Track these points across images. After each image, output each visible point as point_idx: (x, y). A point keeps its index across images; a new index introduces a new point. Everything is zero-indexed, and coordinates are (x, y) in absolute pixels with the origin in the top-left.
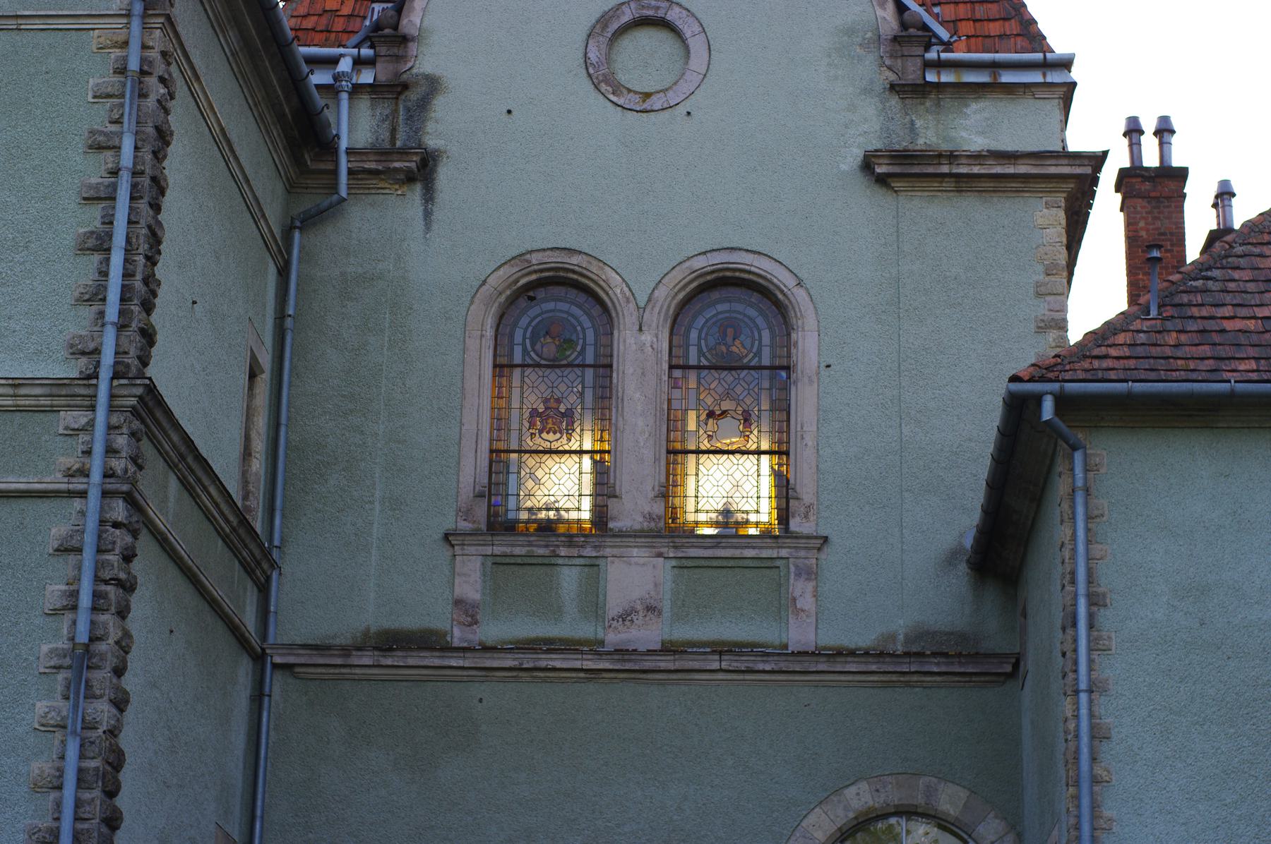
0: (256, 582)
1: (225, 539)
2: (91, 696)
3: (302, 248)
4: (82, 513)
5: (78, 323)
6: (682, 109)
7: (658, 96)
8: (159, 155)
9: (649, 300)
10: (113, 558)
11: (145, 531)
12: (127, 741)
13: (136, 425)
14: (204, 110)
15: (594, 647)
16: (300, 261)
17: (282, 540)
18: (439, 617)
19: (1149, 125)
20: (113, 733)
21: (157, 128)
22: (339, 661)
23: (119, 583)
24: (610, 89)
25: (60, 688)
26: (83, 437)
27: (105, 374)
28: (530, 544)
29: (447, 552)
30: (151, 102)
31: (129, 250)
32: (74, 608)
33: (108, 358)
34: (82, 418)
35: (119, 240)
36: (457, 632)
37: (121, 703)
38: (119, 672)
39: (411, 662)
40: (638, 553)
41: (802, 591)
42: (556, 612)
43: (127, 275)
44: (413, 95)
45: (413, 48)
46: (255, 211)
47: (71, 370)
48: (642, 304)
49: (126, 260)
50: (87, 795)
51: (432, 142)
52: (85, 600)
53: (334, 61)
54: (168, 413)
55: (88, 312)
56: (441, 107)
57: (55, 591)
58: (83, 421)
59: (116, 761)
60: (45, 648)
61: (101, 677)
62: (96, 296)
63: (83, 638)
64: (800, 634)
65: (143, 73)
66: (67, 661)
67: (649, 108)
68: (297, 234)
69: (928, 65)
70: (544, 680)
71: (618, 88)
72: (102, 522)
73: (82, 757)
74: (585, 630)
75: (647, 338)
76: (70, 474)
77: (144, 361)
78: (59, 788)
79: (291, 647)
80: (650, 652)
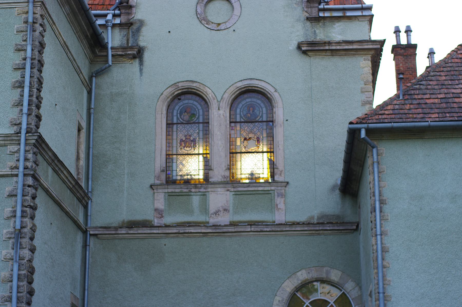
0: (83, 205)
1: (71, 190)
2: (22, 248)
3: (96, 84)
4: (17, 182)
5: (13, 114)
6: (232, 29)
7: (223, 24)
8: (40, 52)
9: (222, 98)
10: (28, 198)
11: (40, 188)
12: (35, 264)
13: (35, 150)
14: (57, 35)
15: (205, 224)
16: (95, 88)
17: (92, 189)
18: (149, 215)
19: (403, 29)
20: (30, 261)
21: (40, 43)
22: (113, 232)
23: (31, 207)
24: (205, 22)
25: (11, 245)
26: (16, 155)
27: (23, 132)
28: (181, 188)
29: (151, 192)
30: (37, 33)
31: (31, 87)
32: (15, 216)
33: (24, 126)
34: (15, 148)
35: (27, 84)
36: (156, 220)
37: (33, 250)
38: (32, 239)
39: (139, 232)
40: (220, 190)
41: (279, 201)
42: (190, 212)
43: (30, 96)
44: (135, 27)
45: (134, 10)
46: (78, 71)
47: (12, 130)
48: (219, 100)
49: (30, 91)
50: (21, 284)
51: (142, 44)
52: (19, 214)
53: (105, 16)
54: (47, 145)
55: (17, 110)
56: (144, 30)
57: (8, 210)
58: (16, 149)
59: (32, 271)
60: (5, 231)
61: (25, 241)
62: (19, 104)
63: (18, 227)
64: (279, 217)
65: (34, 23)
66: (13, 236)
67: (220, 29)
68: (94, 79)
69: (320, 10)
70: (188, 237)
71: (208, 22)
72: (24, 185)
73: (19, 270)
74: (202, 218)
75: (221, 112)
76: (12, 168)
77: (38, 127)
78: (11, 281)
79: (96, 228)
80: (226, 226)
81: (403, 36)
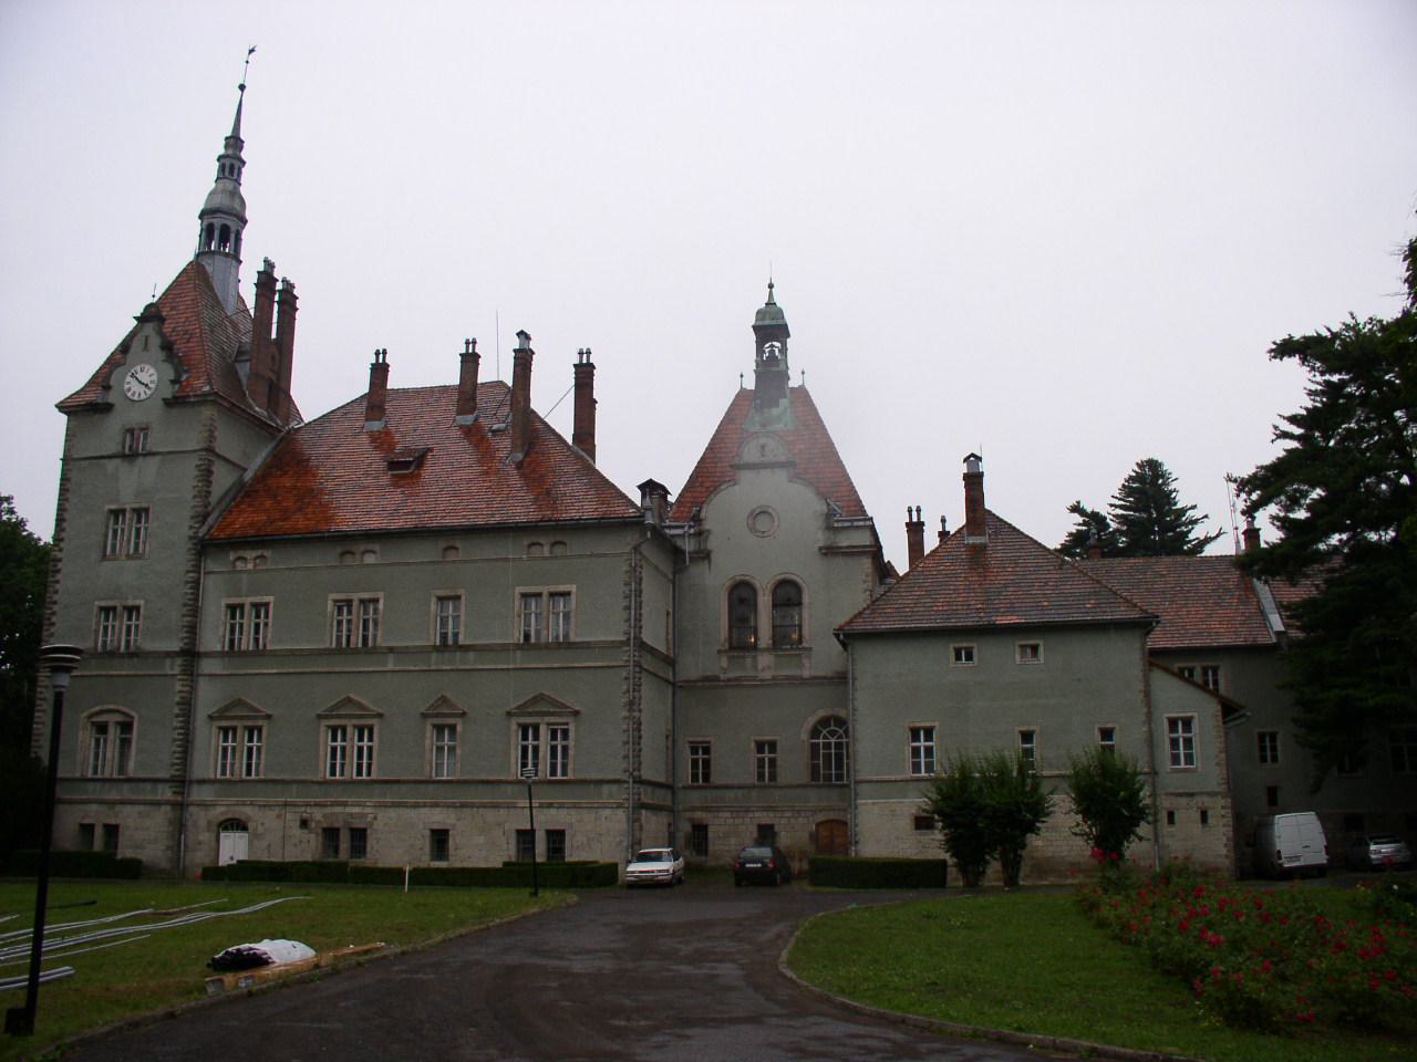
8: (640, 584)
15: (754, 678)
19: (914, 509)
33: (632, 635)
35: (633, 607)
37: (640, 711)
38: (639, 704)
41: (805, 661)
44: (705, 535)
46: (665, 576)
47: (624, 638)
56: (711, 537)
57: (625, 687)
59: (640, 724)
62: (628, 620)
64: (806, 673)
71: (756, 531)
74: (751, 673)
76: (627, 661)
81: (914, 514)
